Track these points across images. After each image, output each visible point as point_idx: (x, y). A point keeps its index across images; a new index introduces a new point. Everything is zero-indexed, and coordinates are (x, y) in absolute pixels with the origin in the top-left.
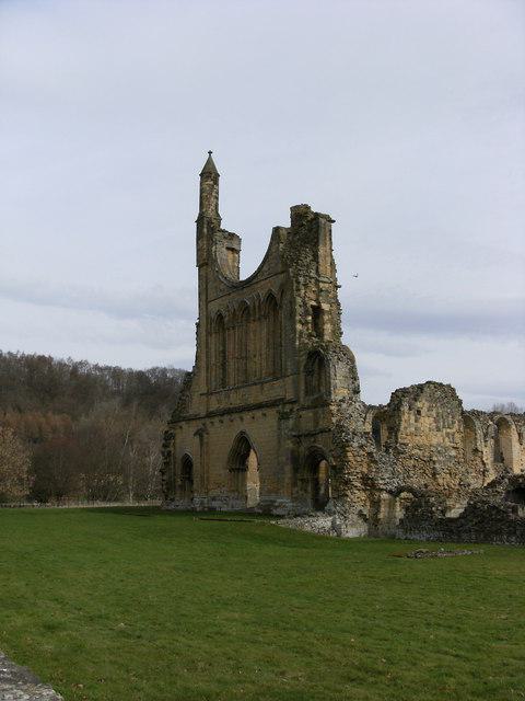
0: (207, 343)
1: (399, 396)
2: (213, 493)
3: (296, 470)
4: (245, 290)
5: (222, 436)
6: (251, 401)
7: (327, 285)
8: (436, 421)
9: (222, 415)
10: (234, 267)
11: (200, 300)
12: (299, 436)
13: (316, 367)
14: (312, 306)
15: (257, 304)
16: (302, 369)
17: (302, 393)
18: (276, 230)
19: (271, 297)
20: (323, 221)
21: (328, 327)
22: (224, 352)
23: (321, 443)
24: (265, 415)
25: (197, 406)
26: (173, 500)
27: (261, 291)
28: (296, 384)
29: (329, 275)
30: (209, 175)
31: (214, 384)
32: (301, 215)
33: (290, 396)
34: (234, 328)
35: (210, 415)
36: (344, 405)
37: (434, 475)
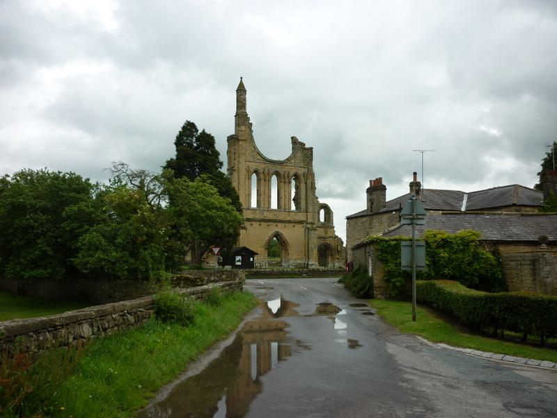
6: (281, 218)
15: (286, 176)
28: (314, 218)
30: (241, 90)
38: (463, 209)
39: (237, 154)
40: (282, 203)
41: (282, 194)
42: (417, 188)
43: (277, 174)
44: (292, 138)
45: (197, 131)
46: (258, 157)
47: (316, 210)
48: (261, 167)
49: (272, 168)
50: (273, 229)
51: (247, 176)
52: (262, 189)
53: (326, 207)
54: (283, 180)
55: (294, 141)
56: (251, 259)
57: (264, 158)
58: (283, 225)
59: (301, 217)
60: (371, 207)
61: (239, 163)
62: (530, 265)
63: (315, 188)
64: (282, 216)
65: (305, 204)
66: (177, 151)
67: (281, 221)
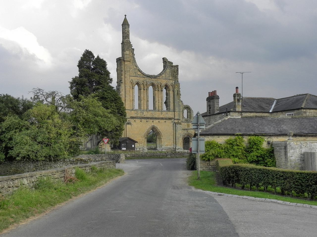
6: (156, 116)
15: (159, 86)
30: (125, 24)
38: (271, 111)
39: (124, 71)
40: (157, 106)
41: (157, 99)
42: (238, 98)
43: (153, 85)
44: (163, 59)
45: (94, 57)
46: (139, 73)
47: (181, 111)
48: (141, 80)
49: (149, 80)
50: (151, 124)
51: (131, 87)
52: (142, 96)
53: (188, 108)
54: (157, 90)
55: (165, 61)
56: (133, 146)
57: (143, 74)
58: (157, 121)
59: (170, 115)
60: (210, 110)
61: (125, 78)
62: (284, 149)
63: (180, 95)
64: (157, 114)
65: (173, 106)
66: (79, 71)
67: (156, 118)
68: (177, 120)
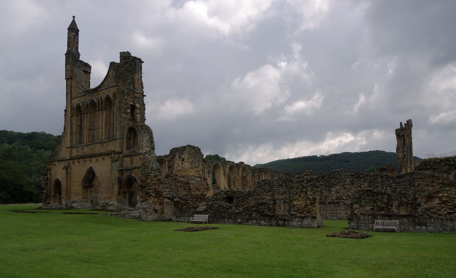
0: (71, 120)
1: (174, 151)
2: (72, 200)
3: (120, 187)
4: (94, 94)
5: (79, 170)
6: (96, 152)
7: (139, 95)
8: (191, 164)
9: (80, 158)
10: (87, 81)
11: (67, 98)
12: (122, 170)
13: (132, 136)
14: (131, 105)
15: (100, 102)
16: (125, 136)
17: (125, 149)
18: (112, 64)
19: (108, 98)
20: (138, 61)
21: (138, 116)
22: (81, 126)
23: (137, 175)
24: (104, 159)
25: (64, 153)
26: (49, 203)
27: (103, 95)
29: (140, 90)
31: (74, 142)
32: (125, 56)
33: (118, 150)
34: (87, 113)
35: (72, 159)
36: (147, 156)
37: (190, 190)
50: (88, 165)
67: (95, 156)
68: (118, 155)
